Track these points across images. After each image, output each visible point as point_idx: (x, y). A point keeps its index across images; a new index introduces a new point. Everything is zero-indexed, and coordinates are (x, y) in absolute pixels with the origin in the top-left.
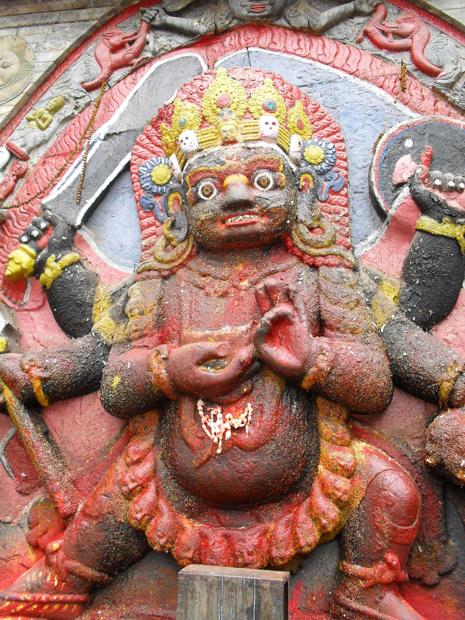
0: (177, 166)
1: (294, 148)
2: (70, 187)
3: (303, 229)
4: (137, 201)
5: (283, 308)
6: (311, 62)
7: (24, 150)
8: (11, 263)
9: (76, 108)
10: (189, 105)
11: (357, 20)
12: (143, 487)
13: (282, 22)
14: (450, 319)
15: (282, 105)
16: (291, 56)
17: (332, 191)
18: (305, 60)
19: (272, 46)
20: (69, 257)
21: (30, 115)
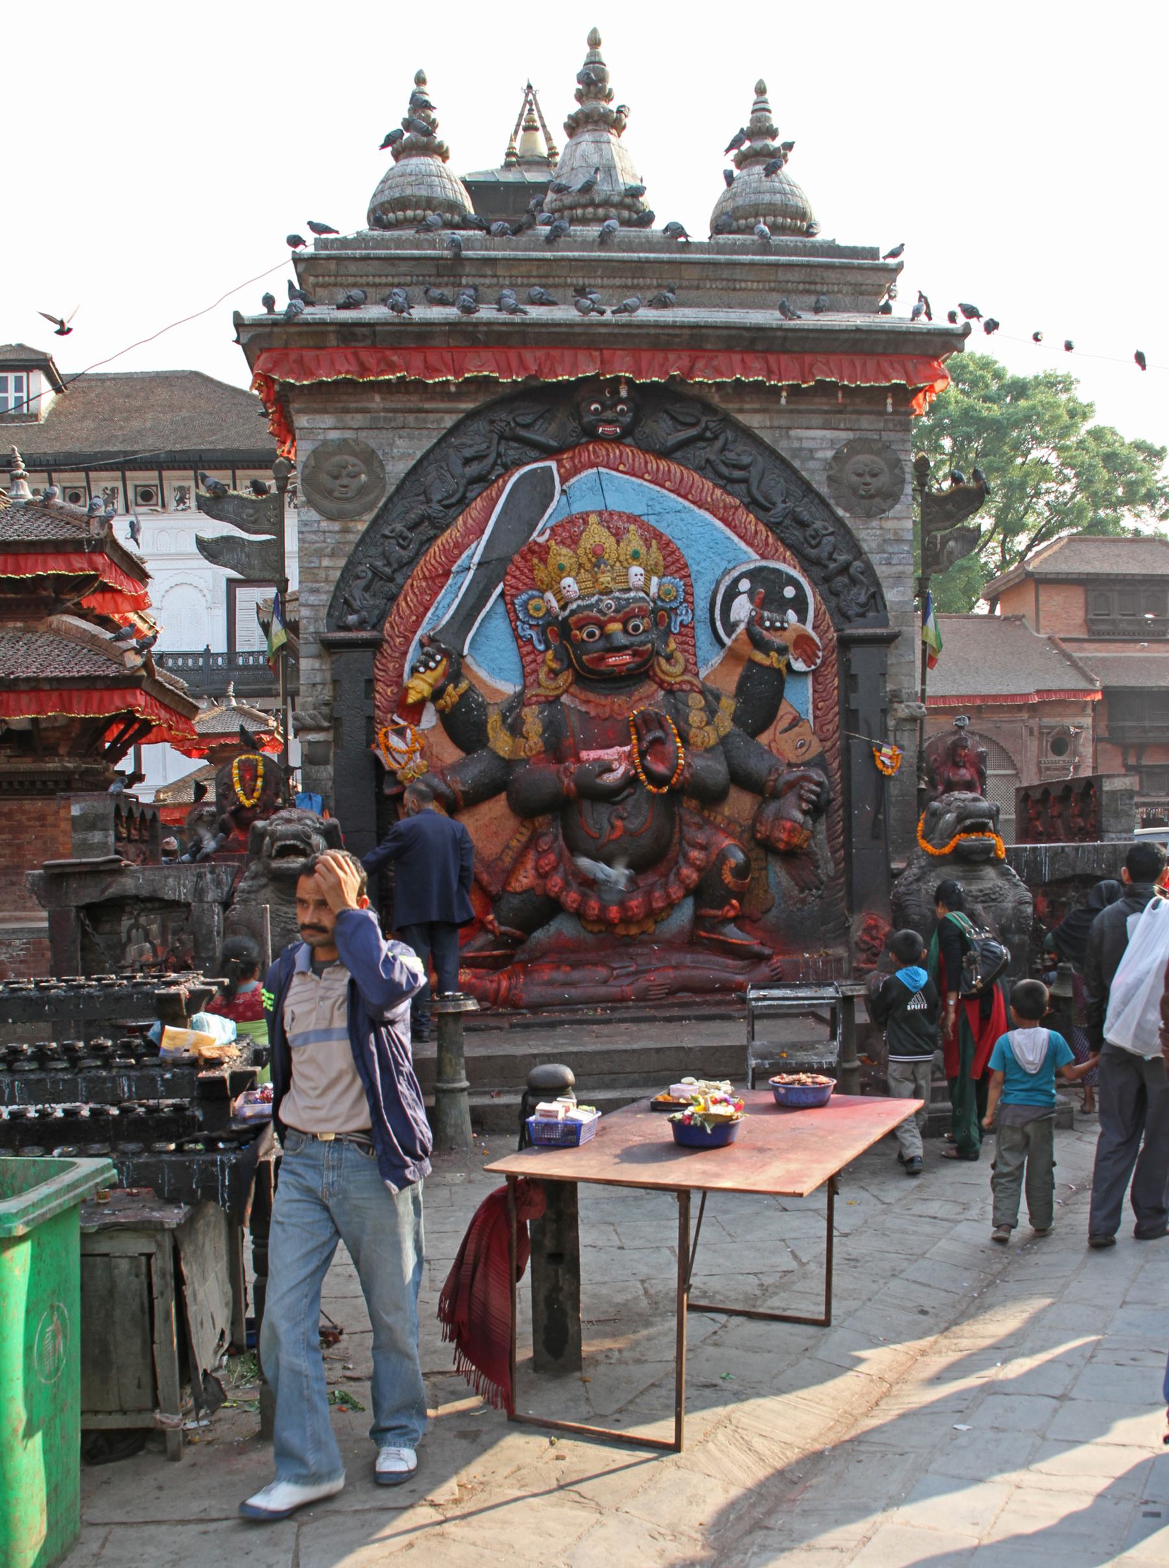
0: (554, 604)
1: (653, 590)
2: (452, 618)
3: (663, 661)
4: (515, 630)
5: (659, 734)
6: (658, 488)
7: (388, 570)
8: (412, 692)
9: (437, 528)
10: (564, 551)
11: (701, 444)
12: (555, 868)
13: (629, 440)
14: (772, 728)
15: (643, 550)
16: (640, 481)
17: (682, 624)
18: (652, 486)
19: (621, 467)
20: (464, 685)
21: (387, 533)
